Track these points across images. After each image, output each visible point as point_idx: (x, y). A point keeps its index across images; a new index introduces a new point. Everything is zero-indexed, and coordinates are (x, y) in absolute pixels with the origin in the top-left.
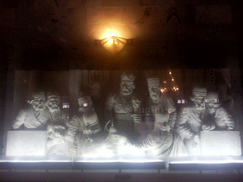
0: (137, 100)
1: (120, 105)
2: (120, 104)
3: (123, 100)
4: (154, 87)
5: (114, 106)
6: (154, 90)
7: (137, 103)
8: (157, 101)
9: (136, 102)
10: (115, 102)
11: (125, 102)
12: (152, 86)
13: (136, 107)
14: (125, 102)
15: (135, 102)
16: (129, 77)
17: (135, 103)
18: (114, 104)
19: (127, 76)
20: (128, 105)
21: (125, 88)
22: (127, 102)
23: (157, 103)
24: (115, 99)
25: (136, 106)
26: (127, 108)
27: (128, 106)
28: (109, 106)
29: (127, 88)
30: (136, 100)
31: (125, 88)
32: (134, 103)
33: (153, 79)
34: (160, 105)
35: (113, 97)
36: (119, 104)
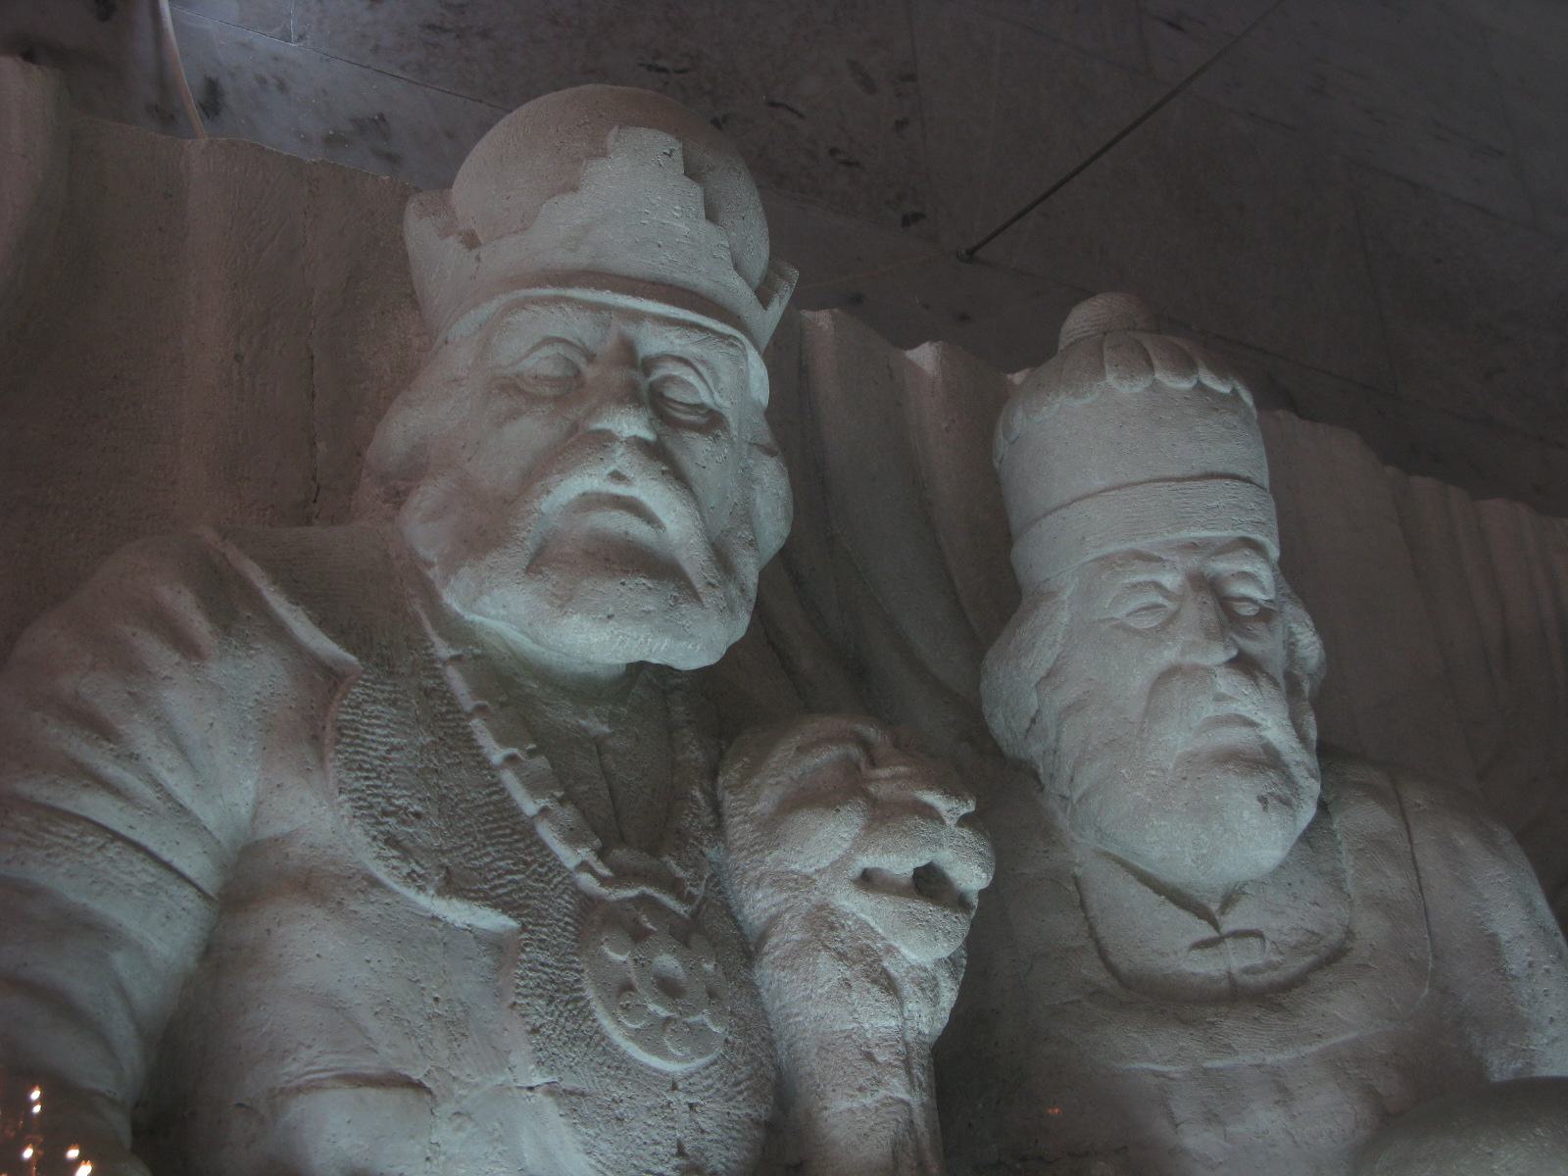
0: (929, 813)
1: (459, 913)
2: (452, 886)
3: (530, 807)
4: (1222, 566)
5: (223, 958)
6: (1253, 647)
7: (929, 884)
8: (1232, 922)
9: (900, 863)
10: (316, 816)
11: (570, 856)
12: (1193, 547)
13: (877, 1019)
14: (570, 856)
15: (868, 880)
16: (712, 215)
17: (854, 904)
18: (252, 883)
19: (693, 172)
20: (668, 962)
21: (621, 459)
22: (622, 876)
23: (1235, 960)
24: (315, 722)
25: (890, 986)
26: (649, 1039)
27: (668, 988)
28: (82, 929)
29: (658, 454)
30: (887, 816)
31: (640, 444)
32: (823, 922)
33: (1201, 387)
34: (1347, 1015)
35: (257, 675)
36: (430, 903)
